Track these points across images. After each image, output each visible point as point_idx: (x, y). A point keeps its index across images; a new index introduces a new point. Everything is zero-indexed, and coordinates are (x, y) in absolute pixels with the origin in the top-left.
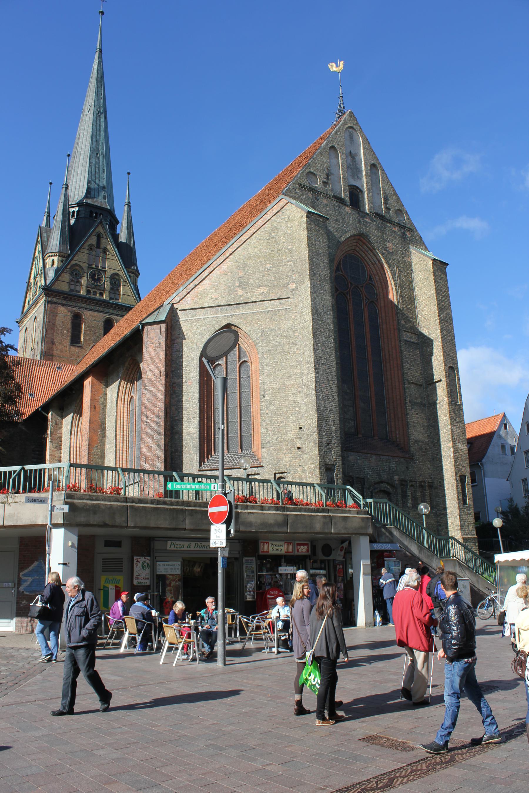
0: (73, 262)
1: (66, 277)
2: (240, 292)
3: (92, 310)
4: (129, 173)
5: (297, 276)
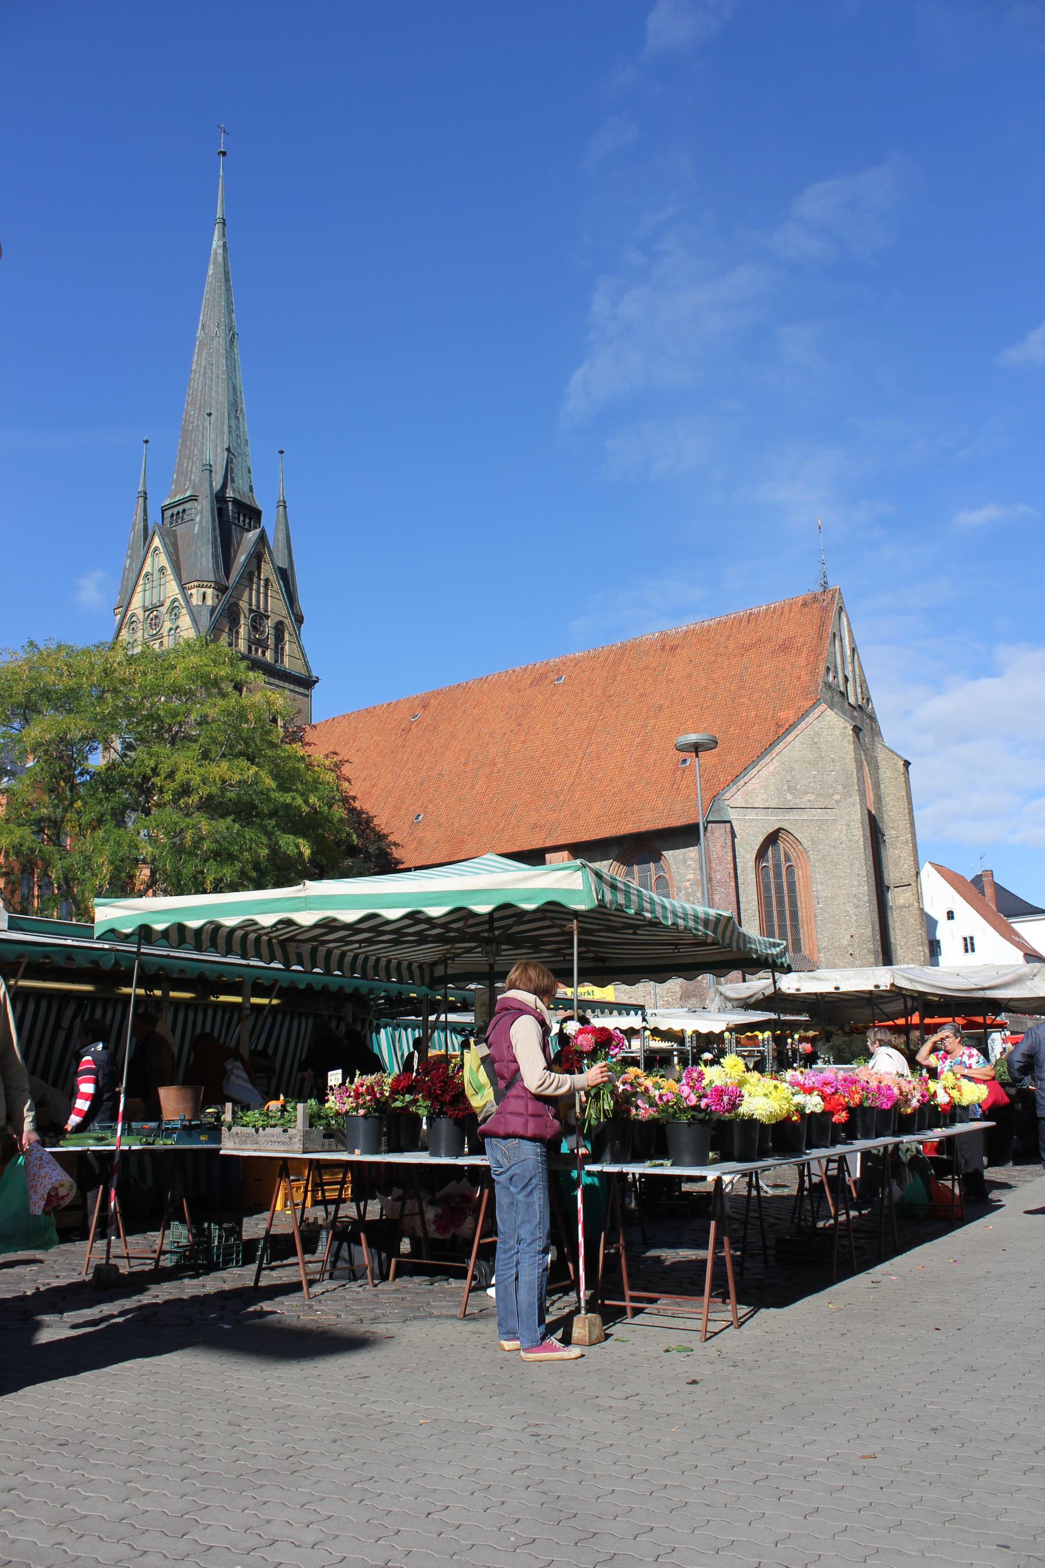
2: (789, 797)
4: (282, 452)
5: (840, 787)
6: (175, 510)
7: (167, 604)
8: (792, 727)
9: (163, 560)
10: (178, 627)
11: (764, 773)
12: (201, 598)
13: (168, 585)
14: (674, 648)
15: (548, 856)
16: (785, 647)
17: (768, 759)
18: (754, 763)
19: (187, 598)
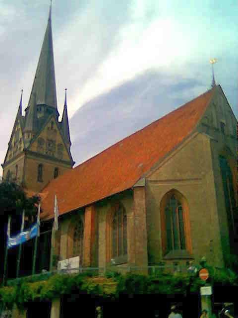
1: (36, 144)
2: (178, 174)
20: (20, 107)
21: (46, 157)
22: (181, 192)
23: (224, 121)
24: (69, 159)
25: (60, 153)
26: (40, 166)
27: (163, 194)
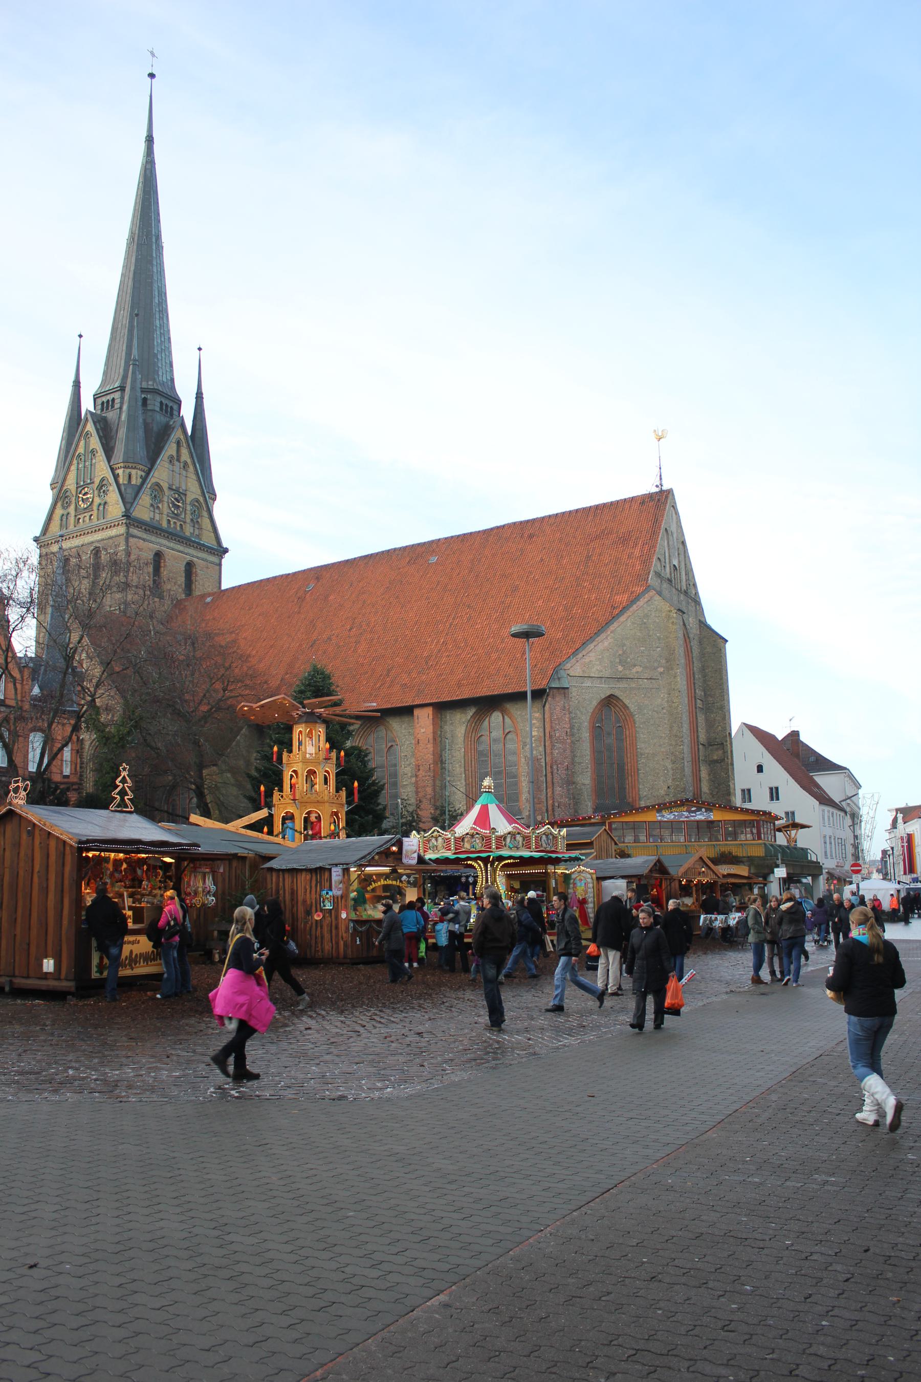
0: (153, 480)
2: (620, 668)
3: (173, 549)
5: (664, 661)
6: (104, 399)
7: (97, 481)
8: (625, 609)
9: (95, 442)
10: (106, 503)
11: (601, 647)
12: (127, 478)
13: (97, 466)
14: (531, 536)
15: (417, 712)
16: (624, 540)
17: (603, 636)
18: (591, 639)
19: (116, 477)
20: (77, 385)
21: (170, 535)
22: (627, 702)
23: (676, 563)
24: (215, 543)
25: (195, 523)
26: (158, 555)
27: (595, 703)
